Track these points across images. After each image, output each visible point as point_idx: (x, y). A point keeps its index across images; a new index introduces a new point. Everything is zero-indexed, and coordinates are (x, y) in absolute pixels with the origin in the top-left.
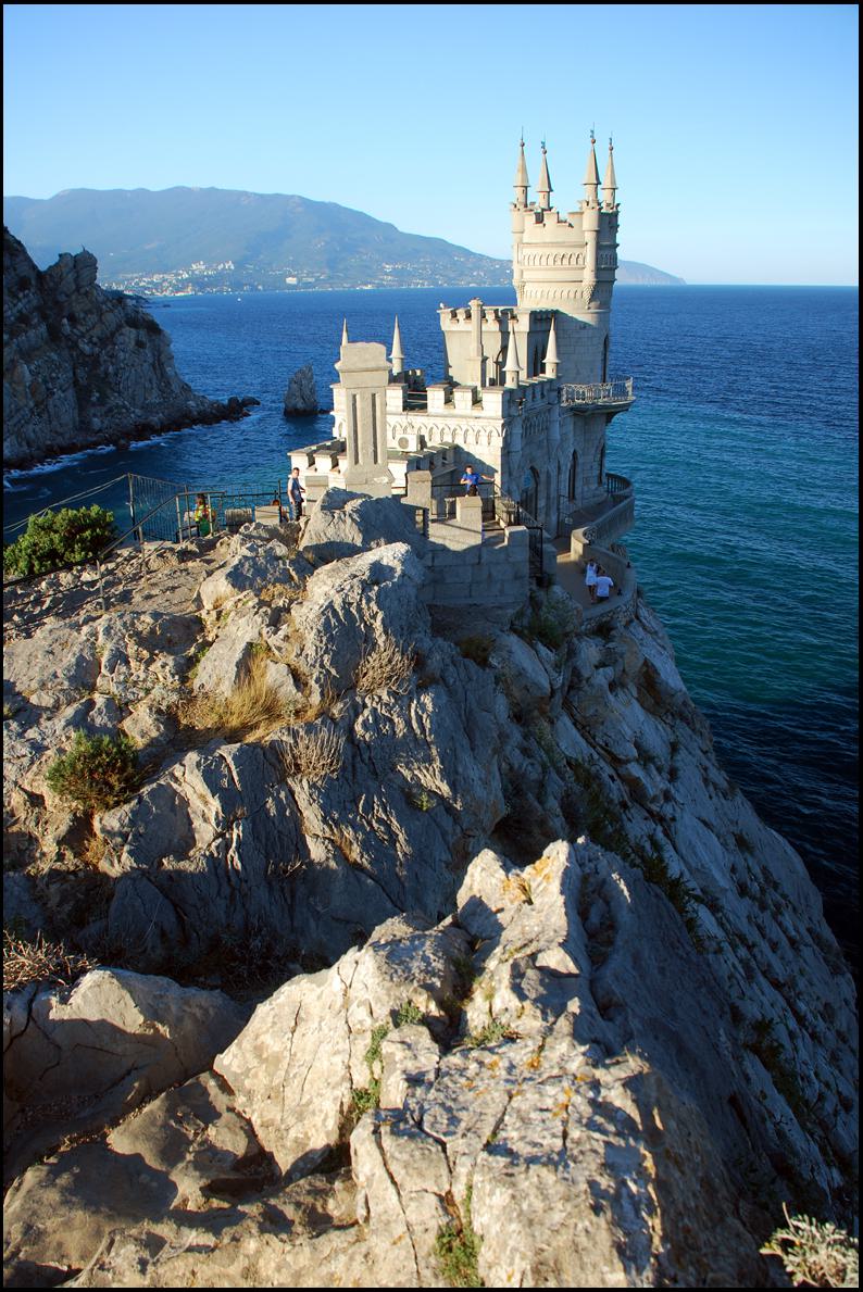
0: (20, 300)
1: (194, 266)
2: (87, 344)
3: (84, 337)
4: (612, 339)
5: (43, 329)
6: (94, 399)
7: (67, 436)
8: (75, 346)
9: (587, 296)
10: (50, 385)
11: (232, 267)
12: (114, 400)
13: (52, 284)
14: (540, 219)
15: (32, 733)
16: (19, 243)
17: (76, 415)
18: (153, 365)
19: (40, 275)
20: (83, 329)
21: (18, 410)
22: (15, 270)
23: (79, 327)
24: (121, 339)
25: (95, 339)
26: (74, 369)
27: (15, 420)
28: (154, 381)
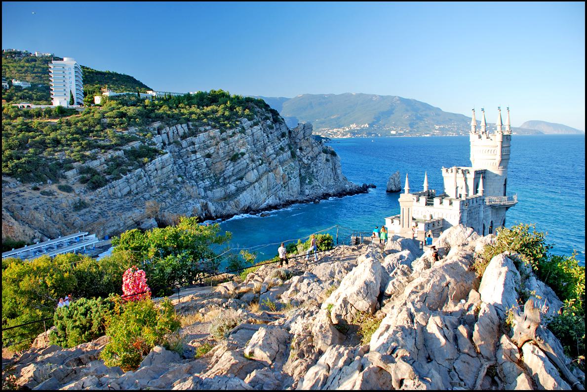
1: (351, 126)
5: (289, 153)
6: (307, 182)
7: (295, 196)
8: (301, 159)
9: (498, 165)
10: (290, 176)
12: (315, 183)
15: (321, 285)
16: (283, 119)
18: (332, 169)
19: (290, 132)
20: (305, 153)
24: (320, 158)
25: (309, 158)
26: (300, 169)
27: (275, 189)
28: (332, 176)
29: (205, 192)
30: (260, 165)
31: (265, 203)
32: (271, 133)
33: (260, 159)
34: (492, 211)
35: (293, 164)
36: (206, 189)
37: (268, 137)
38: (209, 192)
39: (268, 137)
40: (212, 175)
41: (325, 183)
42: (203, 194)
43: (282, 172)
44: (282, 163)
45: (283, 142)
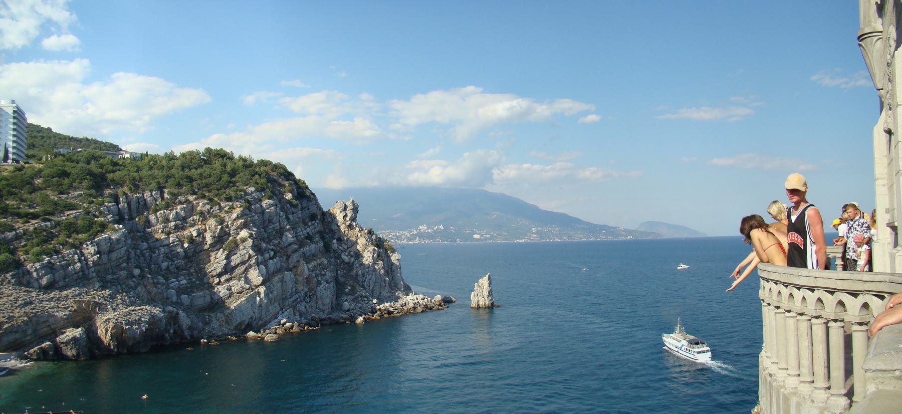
5: (321, 244)
6: (347, 290)
7: (326, 312)
12: (360, 291)
16: (313, 194)
17: (334, 298)
20: (346, 247)
21: (296, 292)
25: (352, 253)
27: (293, 298)
29: (178, 296)
32: (293, 213)
33: (272, 250)
35: (325, 261)
36: (180, 291)
37: (288, 218)
38: (184, 297)
39: (288, 218)
40: (192, 270)
41: (377, 293)
42: (174, 299)
43: (307, 272)
44: (308, 259)
45: (312, 227)
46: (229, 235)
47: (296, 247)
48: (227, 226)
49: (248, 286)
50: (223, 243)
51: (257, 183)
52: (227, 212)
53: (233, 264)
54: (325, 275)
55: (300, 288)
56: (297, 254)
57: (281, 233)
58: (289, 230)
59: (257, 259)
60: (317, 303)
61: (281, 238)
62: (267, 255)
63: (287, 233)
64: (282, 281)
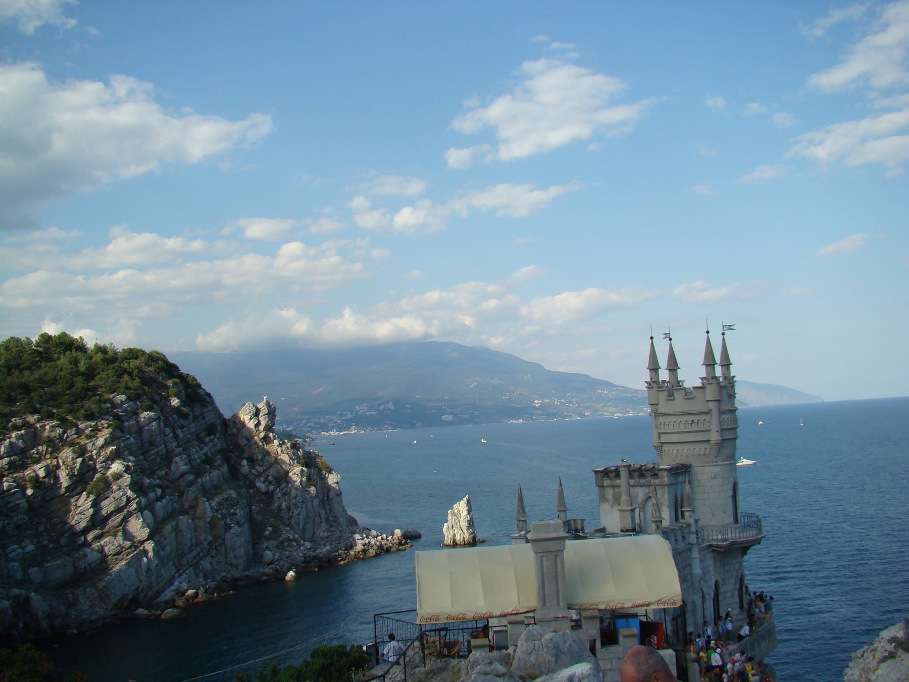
0: (206, 444)
1: (358, 408)
2: (264, 482)
3: (261, 476)
4: (741, 485)
5: (225, 469)
6: (267, 533)
8: (252, 485)
10: (228, 521)
11: (393, 408)
13: (235, 430)
14: (671, 394)
16: (209, 395)
17: (250, 547)
20: (261, 469)
21: (197, 544)
22: (204, 418)
23: (257, 467)
25: (270, 478)
27: (194, 553)
28: (323, 516)
29: (25, 570)
30: (159, 499)
31: (173, 588)
32: (183, 427)
33: (159, 486)
34: (714, 558)
35: (233, 494)
36: (27, 562)
37: (176, 436)
38: (34, 570)
39: (176, 436)
41: (309, 534)
42: (19, 576)
43: (209, 513)
44: (209, 493)
45: (210, 445)
46: (95, 471)
47: (191, 477)
48: (91, 458)
49: (128, 543)
50: (87, 483)
51: (128, 388)
52: (89, 437)
53: (104, 512)
54: (235, 514)
55: (202, 537)
56: (193, 488)
57: (168, 459)
58: (180, 454)
59: (139, 503)
60: (226, 556)
61: (169, 468)
62: (152, 495)
63: (177, 459)
64: (176, 530)
